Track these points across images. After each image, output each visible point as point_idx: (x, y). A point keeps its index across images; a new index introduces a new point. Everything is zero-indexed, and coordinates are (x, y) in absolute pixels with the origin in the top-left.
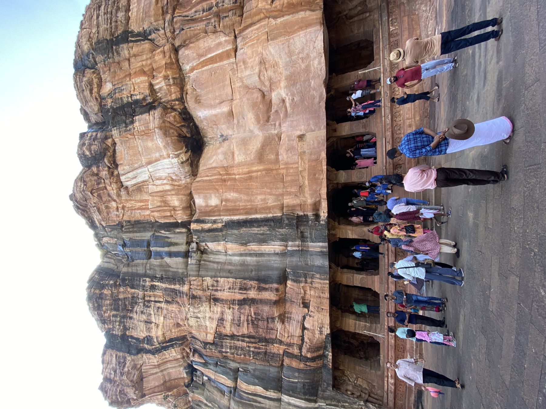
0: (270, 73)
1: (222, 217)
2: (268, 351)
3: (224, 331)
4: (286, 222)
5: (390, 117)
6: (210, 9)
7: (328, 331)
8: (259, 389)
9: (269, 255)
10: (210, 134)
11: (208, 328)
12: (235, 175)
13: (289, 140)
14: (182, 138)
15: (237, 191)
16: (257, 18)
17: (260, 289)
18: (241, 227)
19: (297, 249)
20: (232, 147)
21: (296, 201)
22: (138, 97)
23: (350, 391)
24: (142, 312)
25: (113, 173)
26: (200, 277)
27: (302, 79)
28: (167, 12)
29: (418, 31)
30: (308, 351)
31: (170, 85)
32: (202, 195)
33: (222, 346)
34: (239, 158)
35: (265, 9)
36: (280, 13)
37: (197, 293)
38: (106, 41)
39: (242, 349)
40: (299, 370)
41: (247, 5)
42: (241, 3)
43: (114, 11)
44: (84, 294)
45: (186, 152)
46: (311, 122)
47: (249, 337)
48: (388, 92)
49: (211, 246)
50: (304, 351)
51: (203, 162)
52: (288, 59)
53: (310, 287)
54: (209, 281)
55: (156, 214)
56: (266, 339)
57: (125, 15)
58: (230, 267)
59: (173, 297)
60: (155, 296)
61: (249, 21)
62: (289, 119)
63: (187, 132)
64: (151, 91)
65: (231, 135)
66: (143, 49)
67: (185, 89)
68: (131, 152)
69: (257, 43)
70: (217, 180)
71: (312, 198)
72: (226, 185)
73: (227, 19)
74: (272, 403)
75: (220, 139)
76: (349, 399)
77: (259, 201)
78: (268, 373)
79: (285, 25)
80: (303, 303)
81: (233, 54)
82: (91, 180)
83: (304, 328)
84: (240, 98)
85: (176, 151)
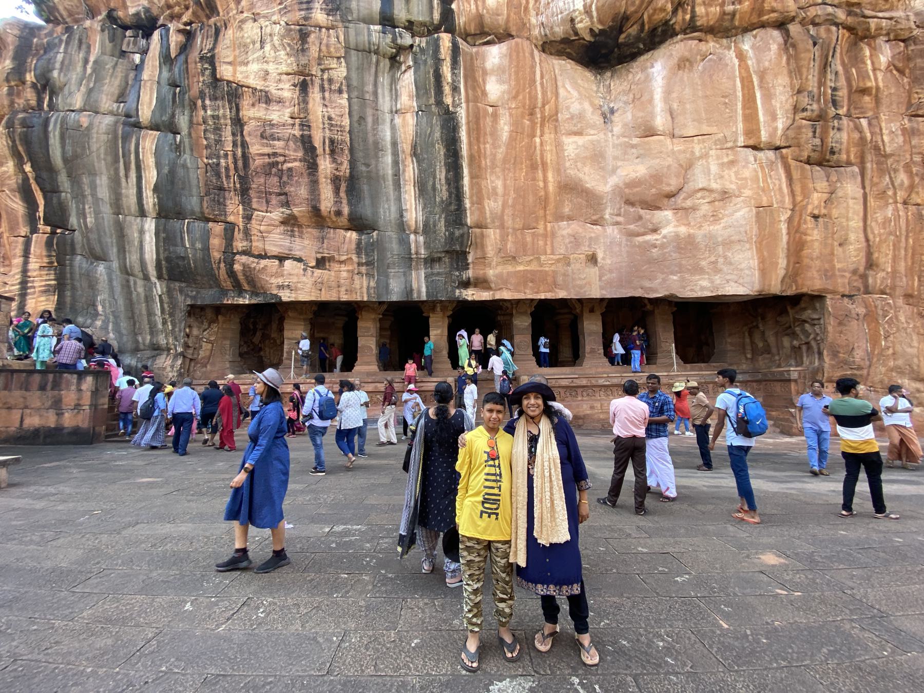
0: (705, 209)
1: (464, 105)
2: (227, 194)
3: (245, 102)
5: (607, 383)
7: (285, 299)
8: (151, 176)
9: (399, 199)
10: (618, 85)
11: (243, 68)
12: (542, 135)
13: (591, 238)
14: (621, 22)
15: (512, 139)
16: (798, 189)
17: (336, 181)
18: (446, 145)
19: (413, 251)
20: (592, 132)
21: (490, 251)
23: (190, 331)
26: (346, 53)
27: (683, 262)
30: (244, 265)
32: (506, 62)
33: (216, 99)
34: (572, 145)
35: (808, 204)
36: (795, 228)
37: (313, 43)
39: (218, 141)
40: (206, 249)
41: (822, 172)
42: (828, 161)
45: (591, 30)
46: (614, 275)
49: (408, 80)
50: (244, 259)
52: (720, 239)
53: (352, 271)
54: (340, 72)
56: (248, 189)
58: (370, 120)
61: (796, 175)
62: (624, 239)
63: (629, 35)
65: (612, 131)
67: (709, 37)
69: (759, 187)
70: (533, 98)
71: (496, 276)
72: (523, 117)
73: (811, 134)
74: (133, 200)
75: (606, 107)
76: (180, 331)
77: (492, 182)
78: (186, 192)
79: (775, 236)
80: (323, 258)
81: (751, 142)
83: (281, 259)
84: (673, 152)
85: (597, 9)
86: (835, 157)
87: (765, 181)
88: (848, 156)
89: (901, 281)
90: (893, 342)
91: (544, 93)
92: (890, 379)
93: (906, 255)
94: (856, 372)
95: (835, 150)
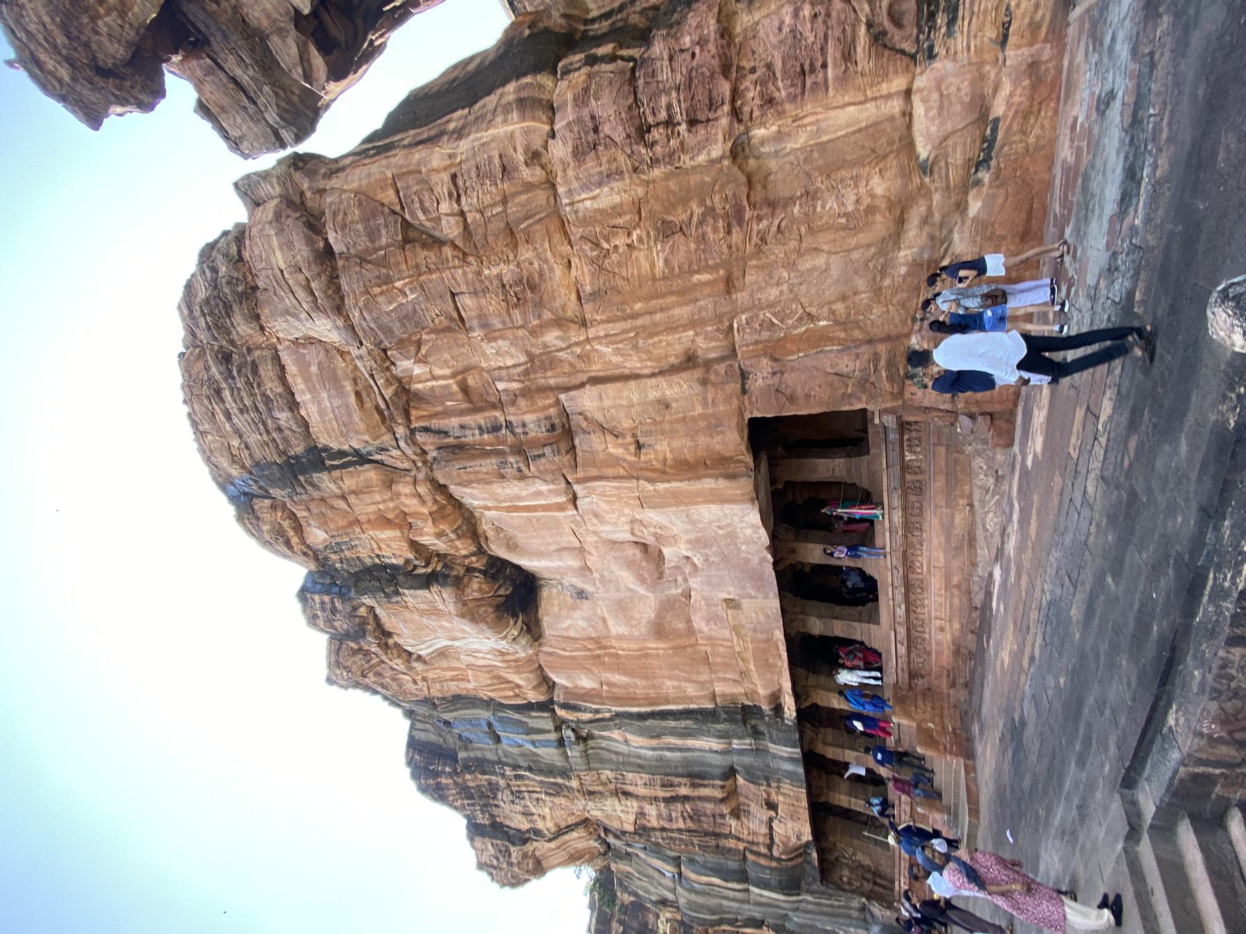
3: (648, 825)
4: (724, 716)
5: (903, 607)
7: (810, 838)
15: (625, 673)
16: (610, 472)
17: (693, 786)
20: (599, 611)
21: (739, 690)
22: (394, 561)
24: (513, 802)
25: (386, 644)
28: (392, 419)
29: (967, 487)
31: (452, 541)
36: (662, 473)
39: (680, 840)
40: (770, 868)
43: (261, 407)
44: (412, 785)
47: (689, 831)
48: (901, 570)
50: (776, 853)
51: (546, 618)
54: (608, 772)
57: (295, 418)
58: (639, 761)
59: (558, 790)
60: (526, 786)
61: (594, 472)
64: (416, 552)
67: (480, 532)
70: (585, 658)
72: (603, 664)
73: (543, 460)
81: (571, 507)
83: (771, 828)
86: (556, 421)
88: (550, 406)
90: (821, 306)
91: (578, 650)
92: (896, 290)
93: (662, 310)
94: (882, 363)
95: (549, 426)
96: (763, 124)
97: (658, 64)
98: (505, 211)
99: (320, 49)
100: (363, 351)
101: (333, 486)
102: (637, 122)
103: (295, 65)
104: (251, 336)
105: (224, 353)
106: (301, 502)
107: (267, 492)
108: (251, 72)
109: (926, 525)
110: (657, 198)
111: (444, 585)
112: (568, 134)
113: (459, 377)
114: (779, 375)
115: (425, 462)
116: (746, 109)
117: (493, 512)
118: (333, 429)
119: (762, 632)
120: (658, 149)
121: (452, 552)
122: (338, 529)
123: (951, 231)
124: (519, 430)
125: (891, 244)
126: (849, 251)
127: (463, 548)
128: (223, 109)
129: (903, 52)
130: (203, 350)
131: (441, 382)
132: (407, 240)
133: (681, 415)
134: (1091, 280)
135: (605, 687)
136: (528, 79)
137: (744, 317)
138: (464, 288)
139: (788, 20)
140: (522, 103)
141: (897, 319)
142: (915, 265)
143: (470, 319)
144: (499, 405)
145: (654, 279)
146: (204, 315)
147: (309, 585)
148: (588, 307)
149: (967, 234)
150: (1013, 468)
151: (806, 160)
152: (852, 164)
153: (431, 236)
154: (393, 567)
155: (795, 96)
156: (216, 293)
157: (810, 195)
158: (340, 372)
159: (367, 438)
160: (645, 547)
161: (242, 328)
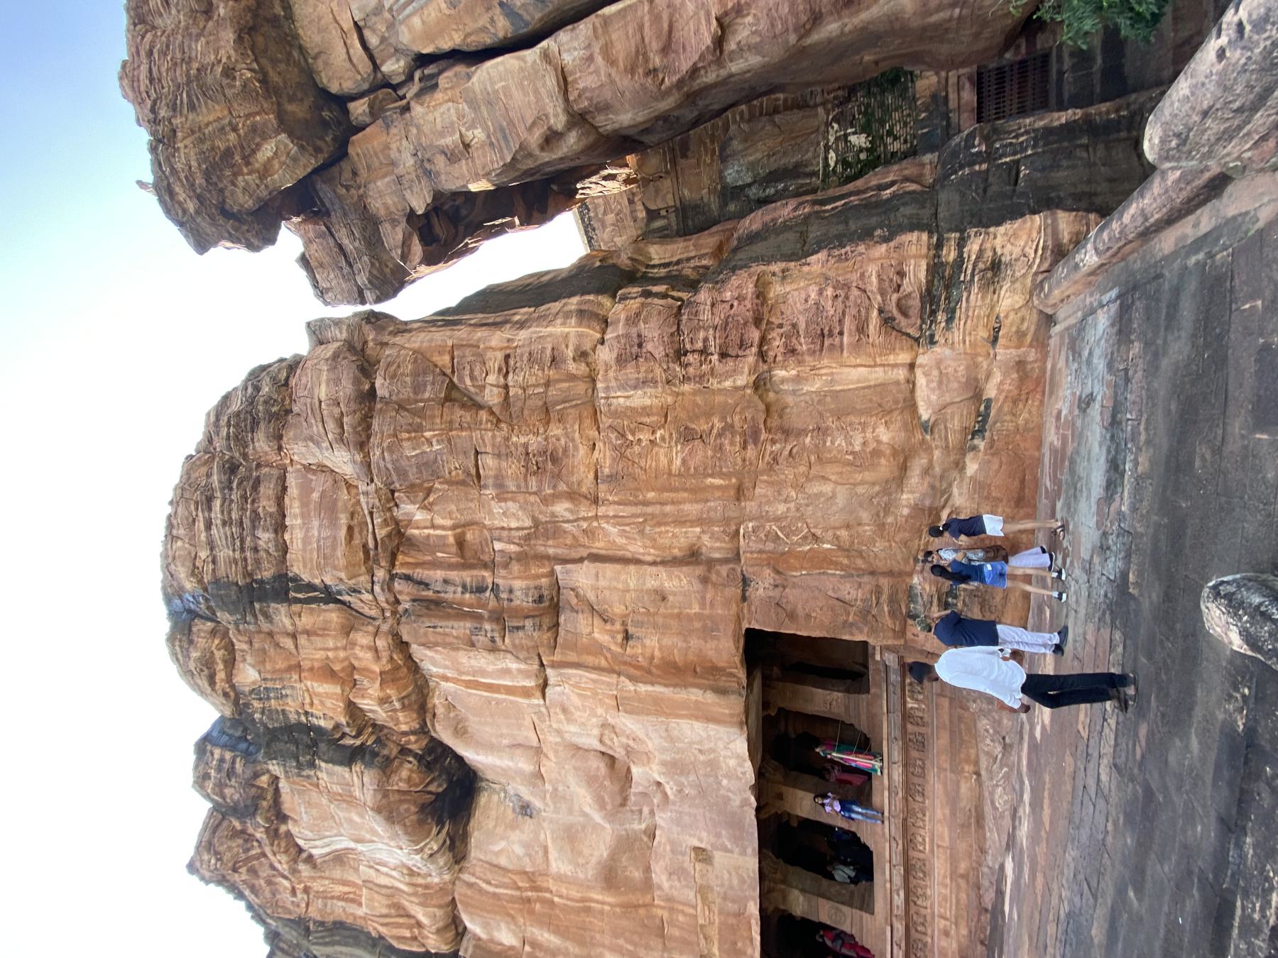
6: (480, 589)
13: (672, 851)
15: (557, 931)
16: (590, 660)
20: (542, 836)
22: (322, 723)
25: (276, 830)
28: (377, 561)
29: (973, 751)
31: (395, 711)
36: (645, 672)
38: (234, 588)
42: (552, 598)
43: (247, 522)
48: (900, 842)
51: (476, 834)
55: (381, 929)
57: (276, 540)
61: (572, 657)
63: (440, 785)
66: (326, 621)
67: (429, 706)
68: (314, 812)
70: (512, 899)
72: (532, 912)
73: (521, 633)
81: (538, 694)
82: (230, 848)
87: (584, 689)
89: (715, 510)
90: (826, 530)
91: (505, 886)
93: (673, 503)
94: (884, 597)
95: (536, 596)
96: (784, 368)
97: (702, 307)
98: (546, 392)
99: (422, 239)
100: (372, 488)
101: (287, 622)
102: (676, 346)
103: (396, 247)
104: (266, 453)
105: (233, 464)
106: (246, 631)
107: (214, 613)
108: (357, 244)
109: (928, 789)
110: (684, 408)
111: (368, 765)
112: (615, 344)
113: (459, 530)
114: (781, 589)
115: (394, 613)
116: (771, 354)
117: (450, 685)
118: (311, 560)
119: (733, 901)
120: (691, 370)
121: (391, 725)
122: (274, 672)
123: (950, 485)
124: (504, 596)
125: (894, 486)
126: (855, 485)
127: (406, 722)
128: (321, 265)
129: (908, 335)
130: (213, 457)
131: (439, 532)
132: (448, 399)
133: (676, 611)
134: (1085, 554)
135: (527, 948)
136: (591, 297)
137: (750, 525)
138: (489, 449)
139: (813, 295)
140: (581, 313)
141: (899, 557)
142: (917, 509)
143: (486, 477)
144: (490, 566)
145: (670, 474)
146: (229, 425)
147: (215, 734)
148: (602, 487)
149: (965, 491)
150: (1022, 738)
151: (819, 402)
152: (861, 413)
153: (472, 399)
154: (319, 730)
155: (814, 352)
156: (249, 409)
157: (821, 431)
158: (340, 504)
159: (343, 575)
160: (612, 760)
161: (261, 444)
